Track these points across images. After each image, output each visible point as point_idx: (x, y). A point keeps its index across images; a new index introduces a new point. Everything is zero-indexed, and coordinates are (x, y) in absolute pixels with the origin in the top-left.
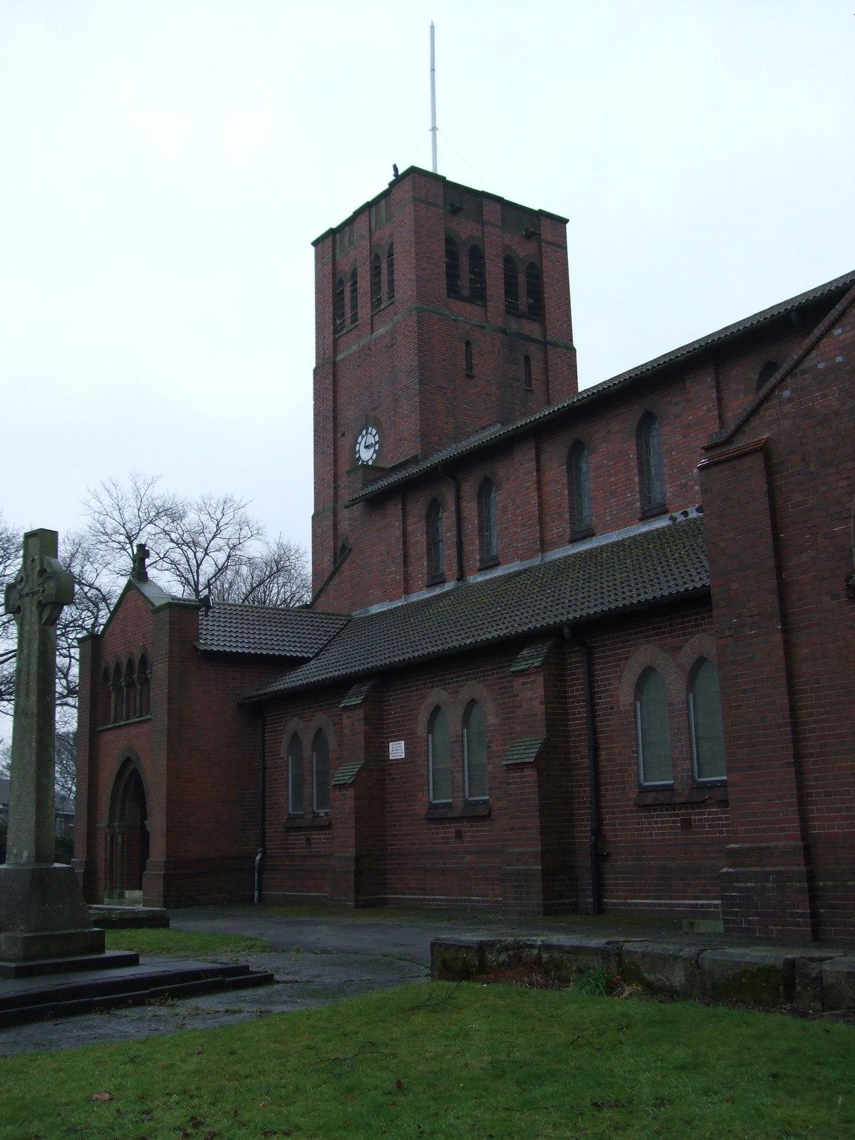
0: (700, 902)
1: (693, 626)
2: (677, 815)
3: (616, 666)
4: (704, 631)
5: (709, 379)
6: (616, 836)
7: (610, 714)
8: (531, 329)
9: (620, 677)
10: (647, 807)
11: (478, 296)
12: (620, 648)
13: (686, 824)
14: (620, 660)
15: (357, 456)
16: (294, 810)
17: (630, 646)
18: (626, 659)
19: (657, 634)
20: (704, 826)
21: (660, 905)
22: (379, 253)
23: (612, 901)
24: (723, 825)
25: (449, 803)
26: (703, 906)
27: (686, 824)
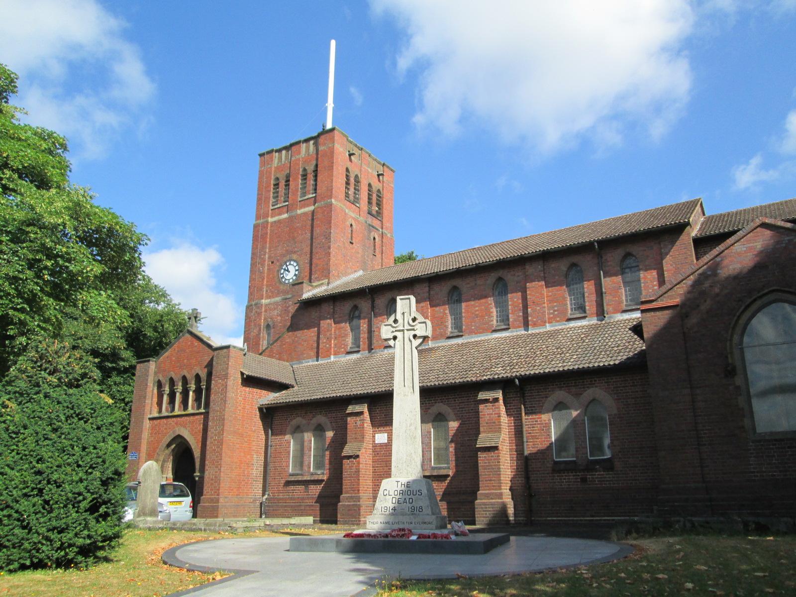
0: (595, 518)
1: (589, 384)
2: (579, 476)
3: (539, 401)
4: (596, 387)
5: (539, 267)
6: (538, 486)
7: (535, 424)
8: (376, 223)
9: (542, 406)
10: (559, 471)
11: (355, 201)
12: (542, 392)
13: (584, 480)
14: (543, 398)
15: (282, 276)
16: (558, 455)
17: (549, 391)
18: (547, 397)
19: (566, 387)
20: (598, 481)
21: (569, 520)
22: (307, 168)
23: (538, 519)
24: (607, 481)
25: (574, 461)
26: (597, 520)
27: (584, 480)
